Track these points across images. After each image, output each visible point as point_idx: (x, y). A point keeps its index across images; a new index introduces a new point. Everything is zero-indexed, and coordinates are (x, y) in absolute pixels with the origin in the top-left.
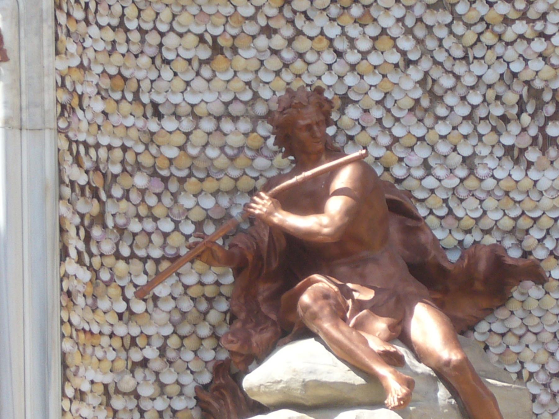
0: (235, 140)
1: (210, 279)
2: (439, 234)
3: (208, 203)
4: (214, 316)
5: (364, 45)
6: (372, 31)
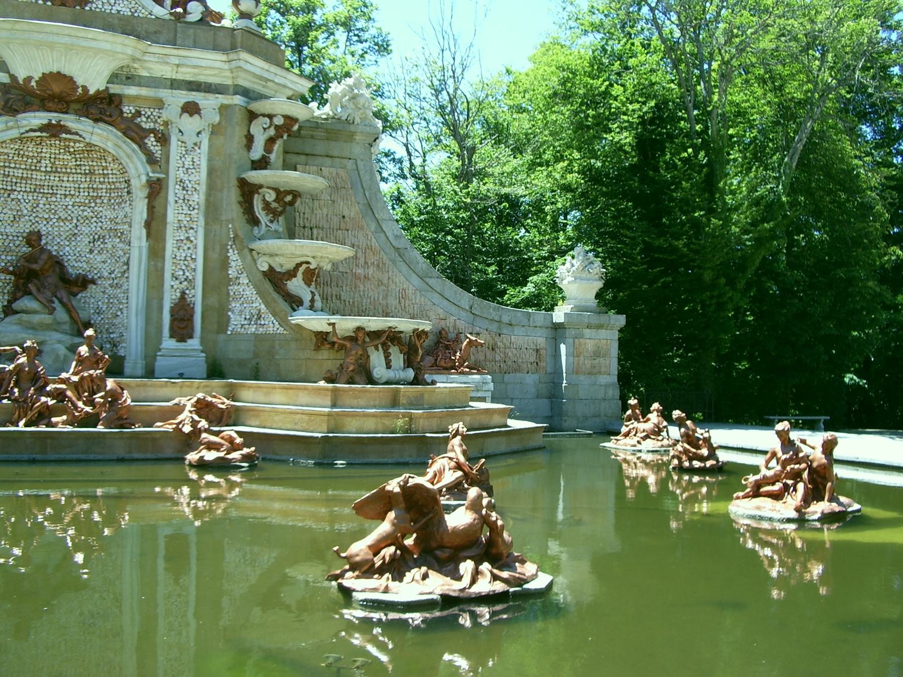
0: (18, 243)
1: (8, 277)
2: (70, 270)
3: (9, 258)
4: (8, 288)
5: (55, 220)
6: (57, 217)
